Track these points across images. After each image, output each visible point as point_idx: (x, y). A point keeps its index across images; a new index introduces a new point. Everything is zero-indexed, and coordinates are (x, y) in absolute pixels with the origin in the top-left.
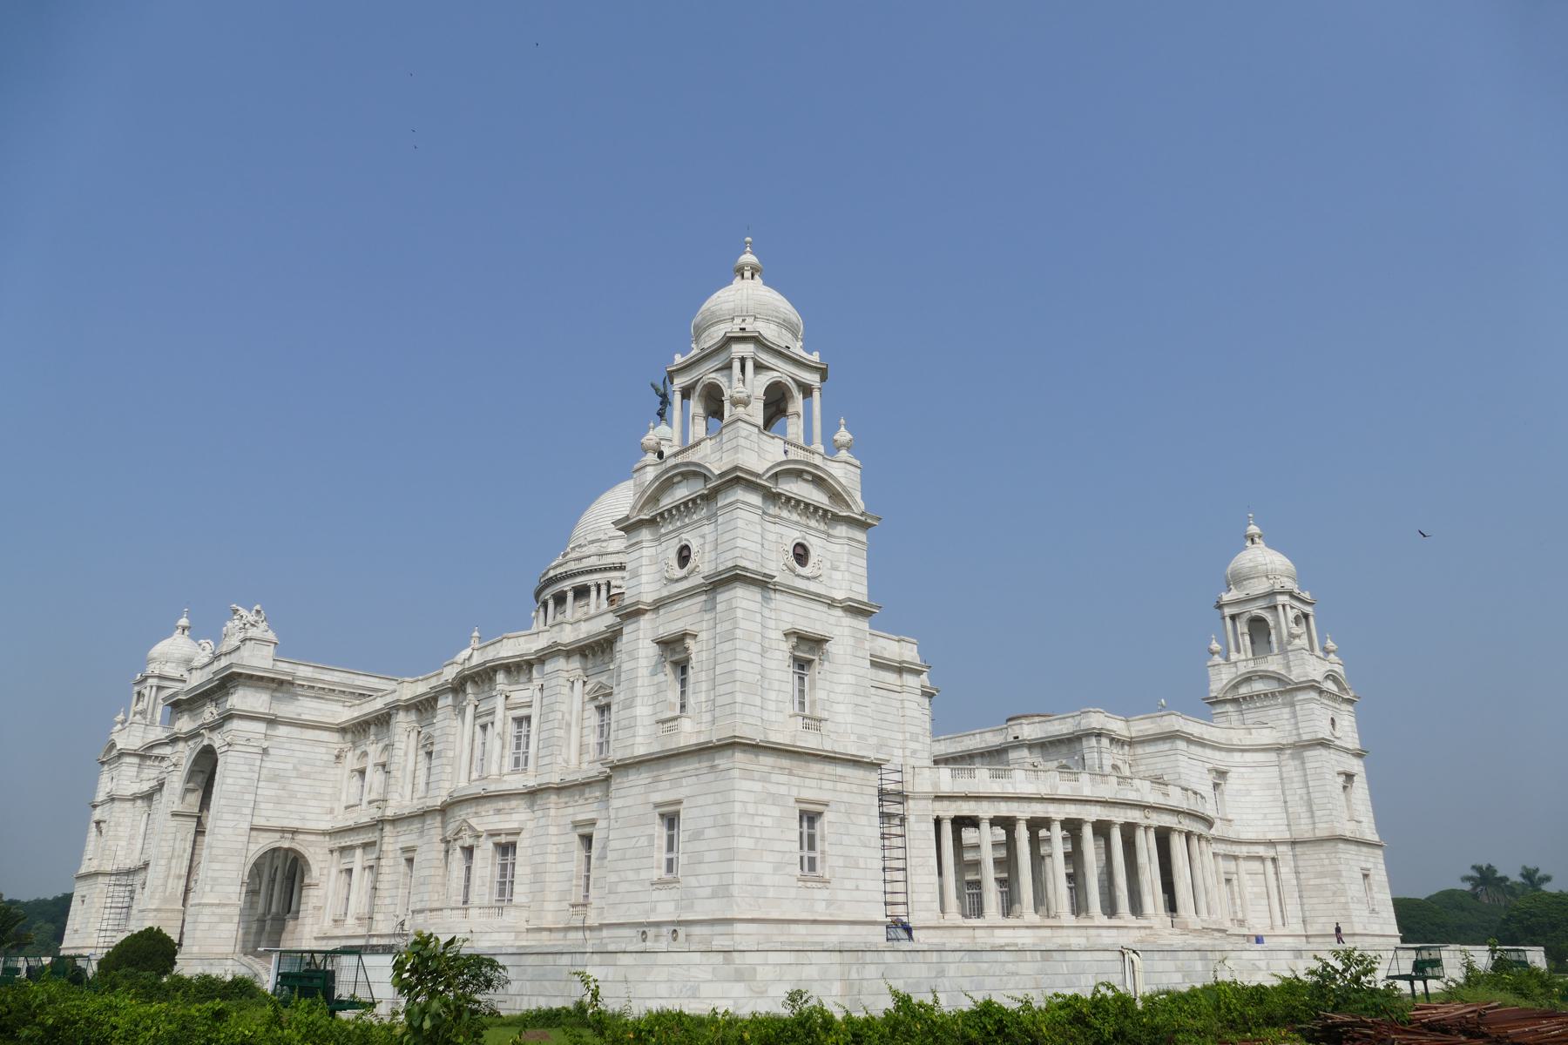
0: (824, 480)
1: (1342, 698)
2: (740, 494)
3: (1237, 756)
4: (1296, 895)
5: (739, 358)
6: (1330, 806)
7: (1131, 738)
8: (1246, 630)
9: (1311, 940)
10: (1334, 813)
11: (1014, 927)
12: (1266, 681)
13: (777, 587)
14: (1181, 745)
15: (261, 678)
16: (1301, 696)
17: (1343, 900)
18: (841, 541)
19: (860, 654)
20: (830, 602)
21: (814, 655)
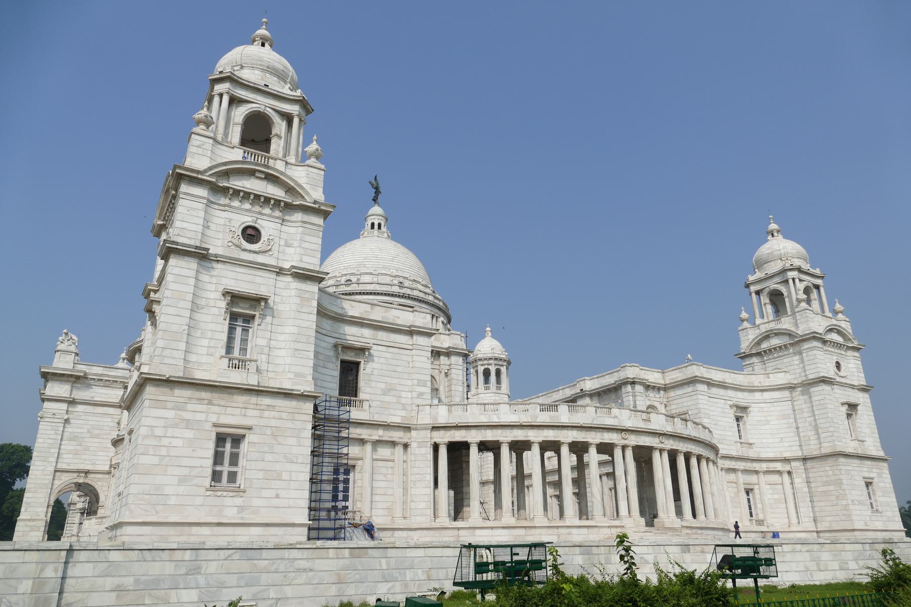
0: (278, 178)
1: (847, 346)
2: (184, 188)
3: (758, 395)
4: (808, 499)
5: (218, 94)
6: (832, 429)
7: (665, 385)
8: (768, 301)
9: (821, 535)
10: (836, 434)
11: (492, 528)
12: (780, 337)
13: (218, 259)
14: (702, 387)
15: (63, 375)
16: (806, 346)
17: (844, 502)
18: (297, 224)
19: (304, 310)
20: (278, 270)
21: (255, 311)
